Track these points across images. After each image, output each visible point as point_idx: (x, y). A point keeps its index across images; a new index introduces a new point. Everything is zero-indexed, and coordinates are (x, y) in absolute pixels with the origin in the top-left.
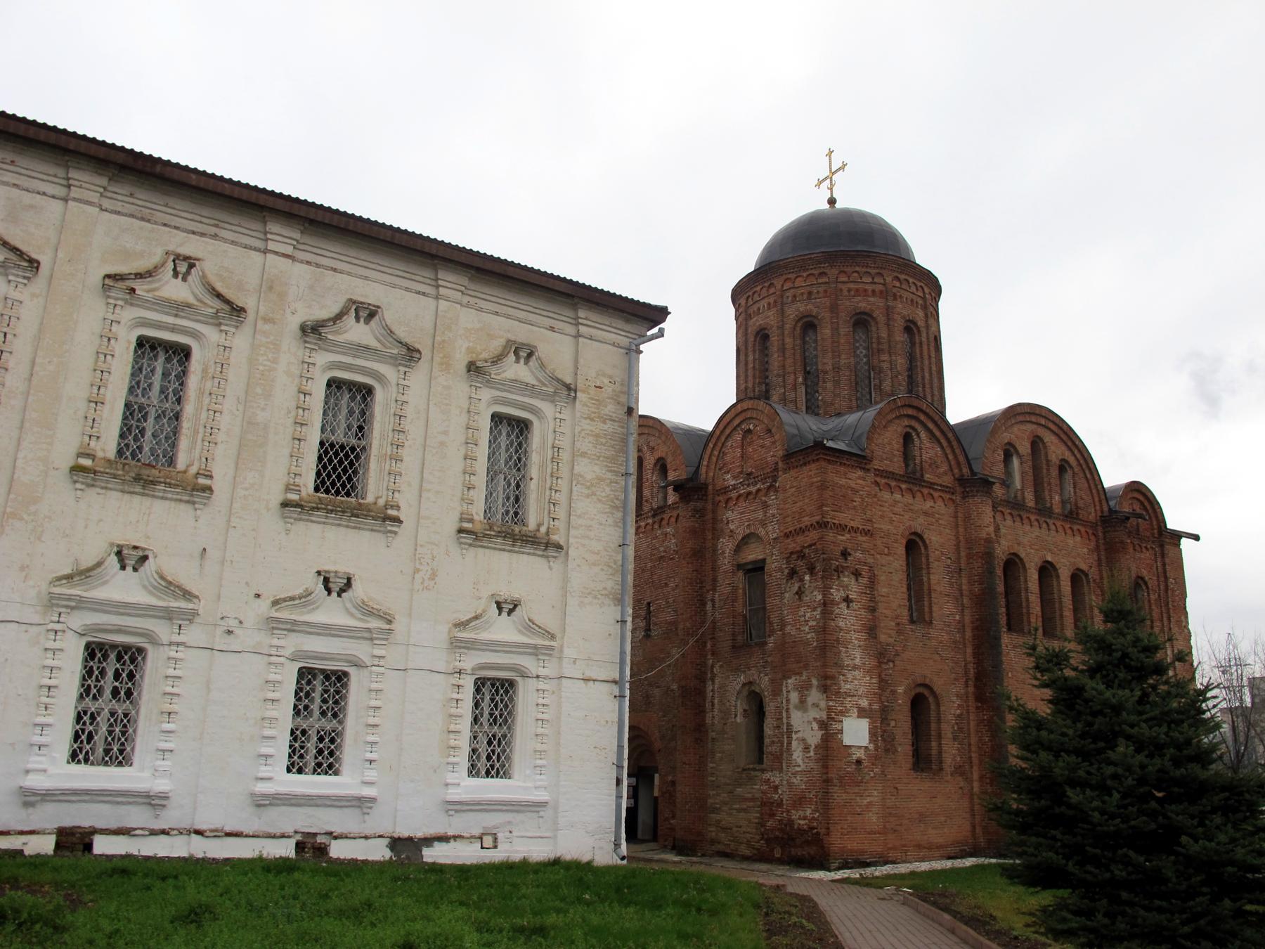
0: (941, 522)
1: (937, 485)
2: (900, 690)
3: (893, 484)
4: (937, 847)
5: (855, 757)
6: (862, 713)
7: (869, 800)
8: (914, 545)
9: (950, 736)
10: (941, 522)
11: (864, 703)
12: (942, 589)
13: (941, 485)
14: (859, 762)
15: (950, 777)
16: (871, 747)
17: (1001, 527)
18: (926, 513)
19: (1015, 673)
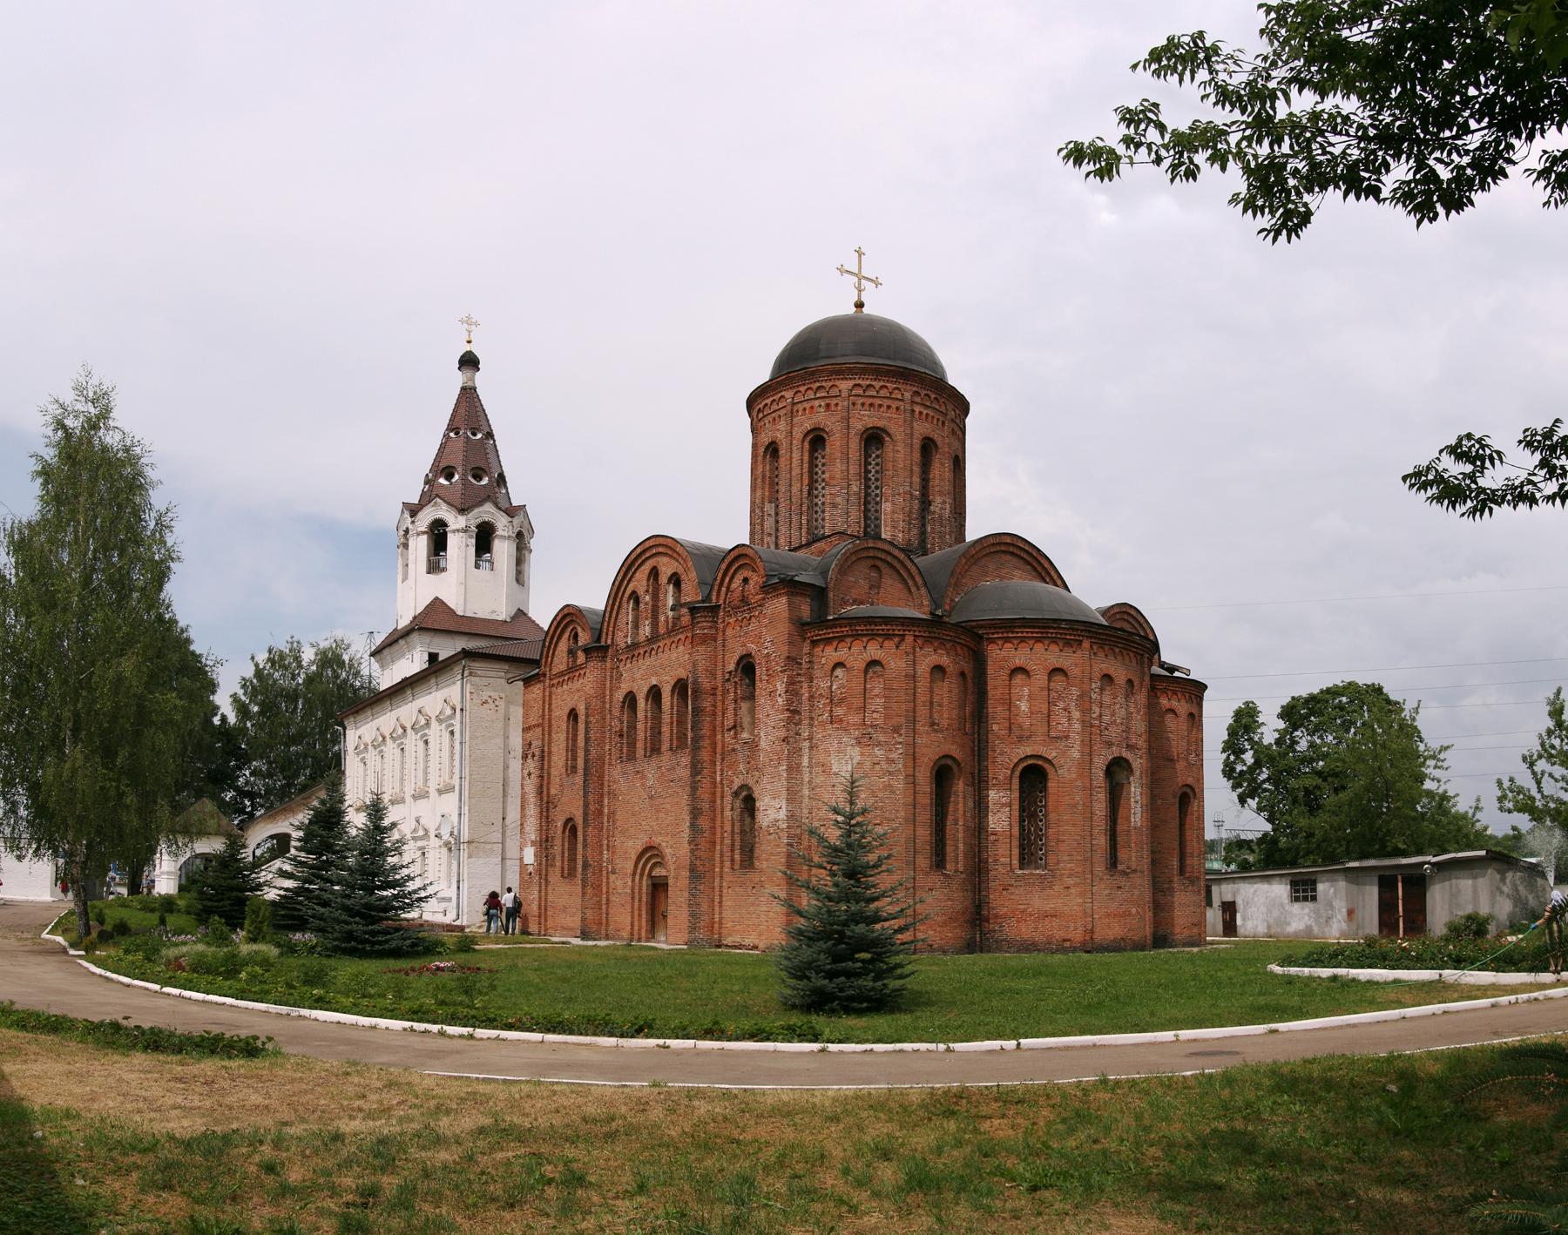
11: (533, 838)
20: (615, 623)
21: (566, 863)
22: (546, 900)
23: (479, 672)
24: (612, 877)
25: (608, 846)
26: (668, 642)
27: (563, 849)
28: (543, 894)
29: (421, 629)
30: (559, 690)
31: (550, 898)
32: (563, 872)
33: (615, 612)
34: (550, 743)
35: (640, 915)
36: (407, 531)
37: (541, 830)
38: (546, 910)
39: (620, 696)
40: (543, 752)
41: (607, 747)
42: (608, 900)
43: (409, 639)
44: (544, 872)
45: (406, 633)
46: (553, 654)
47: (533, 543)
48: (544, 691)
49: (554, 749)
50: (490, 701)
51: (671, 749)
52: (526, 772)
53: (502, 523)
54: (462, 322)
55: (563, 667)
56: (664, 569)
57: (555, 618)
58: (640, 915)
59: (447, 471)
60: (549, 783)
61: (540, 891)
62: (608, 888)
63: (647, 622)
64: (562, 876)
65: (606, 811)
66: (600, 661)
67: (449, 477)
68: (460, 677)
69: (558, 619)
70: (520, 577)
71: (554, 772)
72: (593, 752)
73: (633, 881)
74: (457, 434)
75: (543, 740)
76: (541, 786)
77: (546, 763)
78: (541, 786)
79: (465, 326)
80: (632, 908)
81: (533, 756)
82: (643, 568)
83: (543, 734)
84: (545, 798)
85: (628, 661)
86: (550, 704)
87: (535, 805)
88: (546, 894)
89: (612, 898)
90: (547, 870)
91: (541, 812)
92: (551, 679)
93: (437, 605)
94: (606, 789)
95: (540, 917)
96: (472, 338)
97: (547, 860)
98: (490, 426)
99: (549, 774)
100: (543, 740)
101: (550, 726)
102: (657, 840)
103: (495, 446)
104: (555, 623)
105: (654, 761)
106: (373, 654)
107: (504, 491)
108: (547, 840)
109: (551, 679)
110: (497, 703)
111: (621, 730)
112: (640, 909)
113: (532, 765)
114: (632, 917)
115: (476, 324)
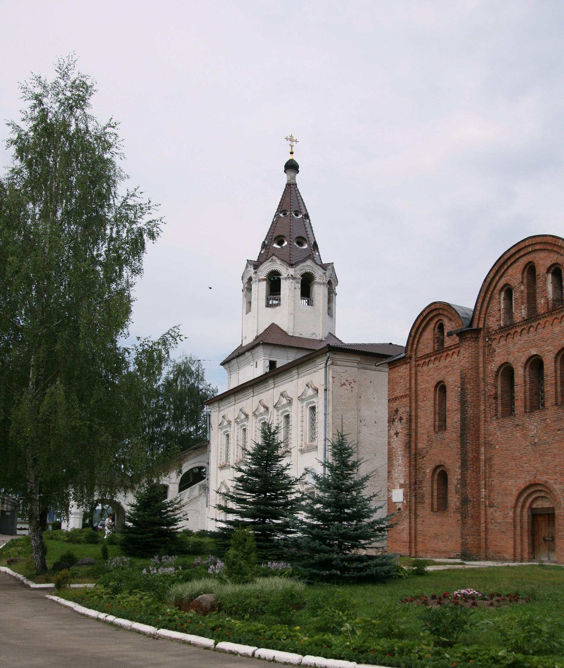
0: (455, 367)
1: (451, 346)
2: (428, 471)
3: (427, 360)
4: (443, 552)
5: (398, 507)
6: (401, 486)
7: (403, 527)
8: (441, 388)
9: (454, 491)
10: (455, 367)
11: (402, 481)
12: (454, 407)
13: (455, 345)
14: (399, 509)
15: (452, 514)
16: (405, 502)
17: (497, 349)
18: (446, 367)
19: (501, 445)
20: (486, 311)
21: (435, 500)
22: (416, 530)
23: (339, 363)
24: (490, 510)
25: (485, 485)
26: (550, 319)
27: (432, 490)
28: (413, 525)
29: (265, 344)
30: (425, 368)
31: (420, 527)
32: (432, 507)
33: (425, 322)
34: (416, 409)
35: (522, 540)
36: (250, 279)
37: (410, 475)
38: (415, 537)
39: (493, 367)
40: (410, 416)
41: (482, 408)
42: (486, 528)
43: (254, 351)
44: (413, 508)
45: (252, 347)
46: (418, 342)
47: (338, 289)
48: (410, 370)
49: (421, 413)
50: (347, 383)
51: (556, 404)
52: (392, 432)
53: (318, 274)
54: (287, 139)
55: (429, 351)
56: (541, 262)
57: (421, 314)
58: (522, 540)
59: (279, 239)
60: (416, 439)
61: (410, 523)
62: (486, 519)
63: (523, 307)
64: (432, 511)
65: (483, 457)
66: (474, 341)
67: (280, 243)
68: (324, 365)
69: (424, 314)
70: (330, 312)
71: (421, 431)
72: (470, 411)
73: (514, 512)
74: (285, 214)
75: (410, 407)
76: (410, 442)
77: (413, 424)
78: (410, 442)
79: (289, 142)
80: (515, 534)
81: (401, 419)
82: (517, 264)
83: (410, 403)
84: (413, 451)
85: (502, 339)
86: (416, 380)
87: (404, 456)
88: (416, 525)
89: (490, 527)
90: (416, 507)
91: (410, 462)
92: (416, 361)
93: (273, 328)
94: (482, 441)
95: (410, 542)
96: (293, 150)
97: (416, 498)
98: (306, 210)
99: (416, 433)
100: (410, 407)
101: (416, 396)
102: (542, 479)
103: (310, 224)
104: (421, 318)
105: (537, 415)
106: (222, 364)
107: (317, 254)
108: (415, 483)
109: (416, 361)
110: (352, 385)
111: (496, 394)
112: (521, 535)
113: (399, 426)
114: (515, 542)
115: (296, 141)
